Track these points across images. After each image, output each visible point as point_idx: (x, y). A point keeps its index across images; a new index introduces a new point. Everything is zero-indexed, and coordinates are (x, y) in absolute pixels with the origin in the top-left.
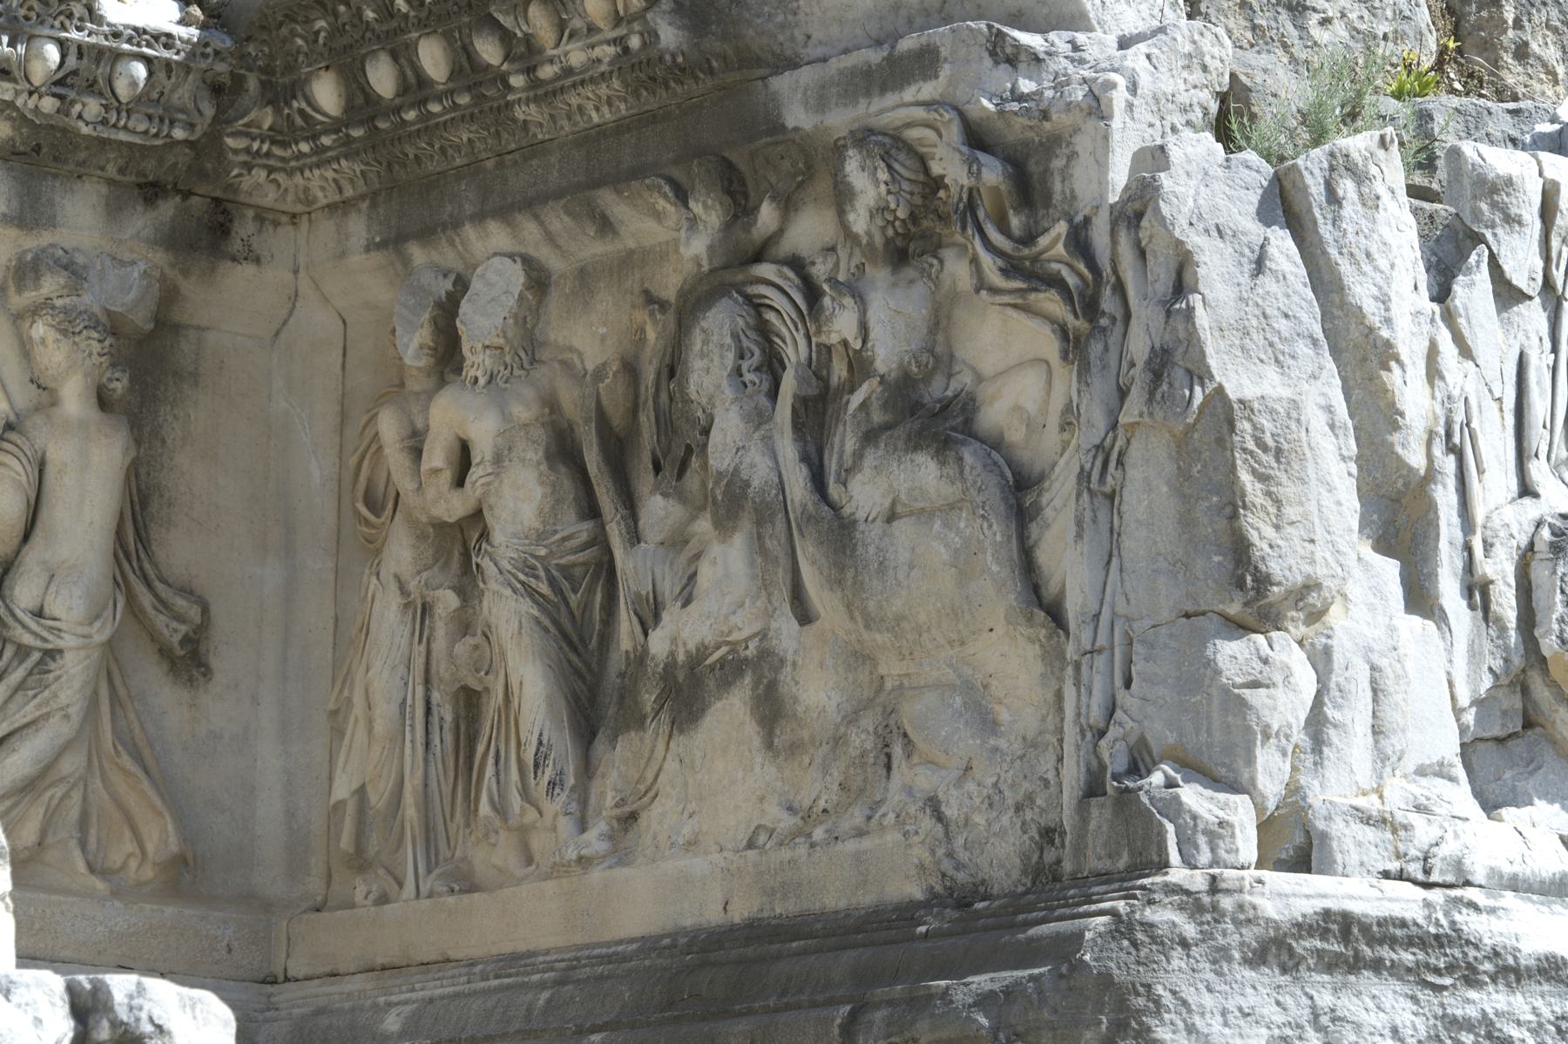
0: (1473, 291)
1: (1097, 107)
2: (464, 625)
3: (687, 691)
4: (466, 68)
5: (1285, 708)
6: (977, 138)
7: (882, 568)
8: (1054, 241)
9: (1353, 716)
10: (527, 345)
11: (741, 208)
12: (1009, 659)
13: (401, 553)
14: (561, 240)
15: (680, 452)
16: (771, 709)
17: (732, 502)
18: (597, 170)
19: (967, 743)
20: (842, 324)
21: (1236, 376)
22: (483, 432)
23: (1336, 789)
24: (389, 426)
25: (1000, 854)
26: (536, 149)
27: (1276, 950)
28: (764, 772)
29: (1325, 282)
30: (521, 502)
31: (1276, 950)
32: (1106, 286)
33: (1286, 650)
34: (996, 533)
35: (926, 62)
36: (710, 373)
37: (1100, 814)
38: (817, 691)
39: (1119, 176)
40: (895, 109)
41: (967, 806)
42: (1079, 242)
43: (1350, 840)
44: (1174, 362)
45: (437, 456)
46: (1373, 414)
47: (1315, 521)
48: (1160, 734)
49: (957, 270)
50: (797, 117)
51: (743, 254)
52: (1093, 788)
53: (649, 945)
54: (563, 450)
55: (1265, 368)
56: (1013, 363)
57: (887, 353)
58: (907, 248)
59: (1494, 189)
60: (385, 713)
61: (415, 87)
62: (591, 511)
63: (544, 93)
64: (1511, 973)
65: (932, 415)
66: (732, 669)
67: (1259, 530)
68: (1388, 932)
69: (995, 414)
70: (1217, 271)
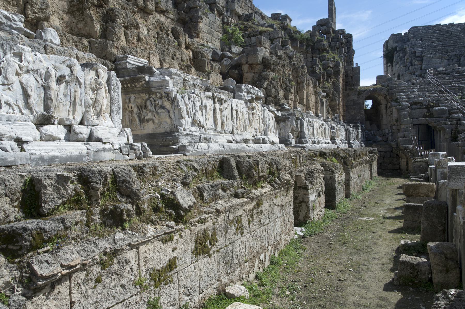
0: (190, 101)
1: (172, 92)
2: (131, 116)
3: (148, 121)
4: (131, 86)
5: (184, 123)
6: (165, 93)
7: (387, 179)
8: (170, 99)
9: (187, 123)
10: (135, 101)
11: (149, 95)
12: (168, 121)
13: (127, 112)
14: (137, 96)
15: (146, 107)
16: (153, 122)
17: (150, 111)
18: (140, 92)
19: (166, 124)
20: (157, 102)
21: (181, 106)
22: (133, 106)
23: (186, 127)
24: (126, 105)
25: (168, 130)
26: (135, 91)
27: (185, 135)
28: (153, 125)
29: (185, 101)
30: (136, 110)
31: (185, 135)
32: (174, 101)
33: (184, 120)
35: (162, 89)
36: (148, 103)
37: (175, 129)
38: (156, 121)
39: (173, 96)
40: (160, 91)
41: (166, 127)
42: (171, 99)
43: (187, 130)
44: (178, 106)
45: (130, 107)
46: (187, 108)
47: (184, 114)
48: (178, 125)
49: (164, 100)
50: (153, 91)
51: (150, 98)
52: (174, 127)
53: (147, 134)
54: (138, 107)
55: (182, 106)
56: (167, 105)
57: (160, 104)
58: (161, 98)
59: (191, 96)
60: (127, 121)
61: (128, 87)
62: (140, 110)
63: (136, 88)
64: (195, 136)
65: (163, 107)
66: (151, 120)
67: (182, 114)
68: (189, 134)
69: (167, 107)
70: (180, 101)
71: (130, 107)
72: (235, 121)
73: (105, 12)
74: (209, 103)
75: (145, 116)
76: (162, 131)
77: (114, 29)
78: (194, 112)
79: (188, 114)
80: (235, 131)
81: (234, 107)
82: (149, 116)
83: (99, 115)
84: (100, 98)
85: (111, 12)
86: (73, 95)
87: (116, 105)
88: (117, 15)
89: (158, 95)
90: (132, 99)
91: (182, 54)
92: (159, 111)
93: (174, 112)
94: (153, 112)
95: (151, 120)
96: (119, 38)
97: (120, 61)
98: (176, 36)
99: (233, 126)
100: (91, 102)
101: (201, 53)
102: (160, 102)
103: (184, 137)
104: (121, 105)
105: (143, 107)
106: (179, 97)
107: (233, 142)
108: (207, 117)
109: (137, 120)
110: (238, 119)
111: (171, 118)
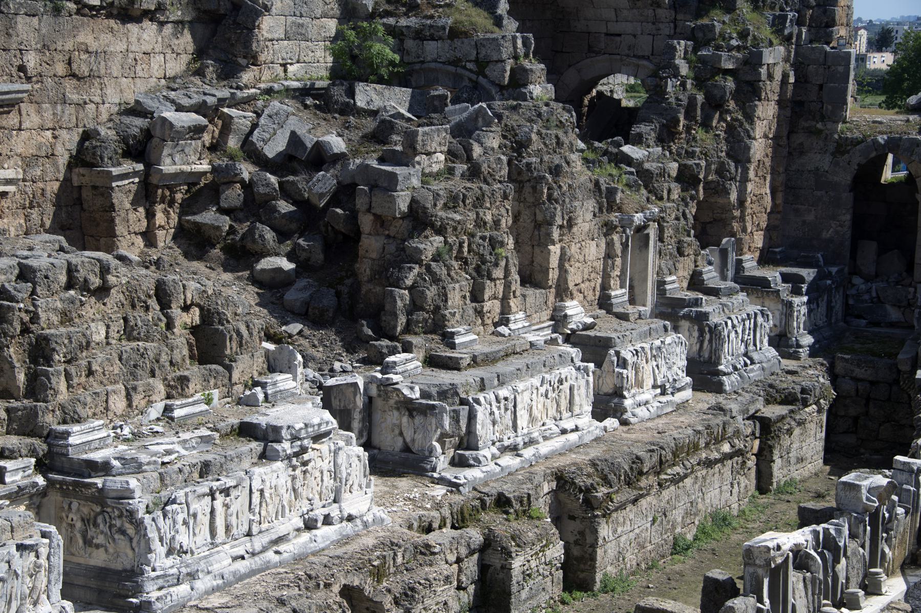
2: (71, 532)
3: (98, 546)
4: (74, 490)
5: (153, 560)
10: (78, 510)
11: (103, 507)
12: (130, 553)
15: (96, 525)
16: (106, 551)
17: (102, 532)
21: (150, 535)
22: (75, 519)
23: (157, 564)
25: (128, 567)
29: (156, 525)
30: (79, 525)
32: (139, 524)
34: (129, 544)
36: (100, 520)
38: (111, 550)
41: (125, 561)
43: (158, 569)
44: (145, 535)
45: (70, 519)
46: (159, 533)
54: (83, 520)
55: (152, 534)
56: (131, 531)
57: (118, 525)
58: (120, 516)
64: (169, 576)
65: (123, 532)
66: (102, 546)
71: (70, 519)
72: (257, 510)
73: (34, 340)
74: (201, 507)
75: (93, 538)
76: (119, 567)
77: (49, 379)
78: (173, 533)
79: (161, 540)
80: (255, 530)
81: (256, 485)
82: (100, 540)
83: (35, 604)
84: (38, 584)
85: (43, 343)
86: (9, 592)
87: (56, 572)
88: (54, 350)
89: (117, 513)
90: (75, 505)
91: (172, 351)
92: (116, 536)
93: (139, 542)
94: (106, 534)
95: (102, 546)
96: (56, 393)
97: (56, 437)
98: (164, 301)
99: (251, 522)
100: (28, 592)
101: (218, 314)
102: (118, 523)
103: (151, 583)
104: (62, 571)
105: (91, 521)
106: (147, 519)
107: (246, 556)
108: (197, 531)
109: (81, 542)
110: (264, 505)
111: (133, 549)
